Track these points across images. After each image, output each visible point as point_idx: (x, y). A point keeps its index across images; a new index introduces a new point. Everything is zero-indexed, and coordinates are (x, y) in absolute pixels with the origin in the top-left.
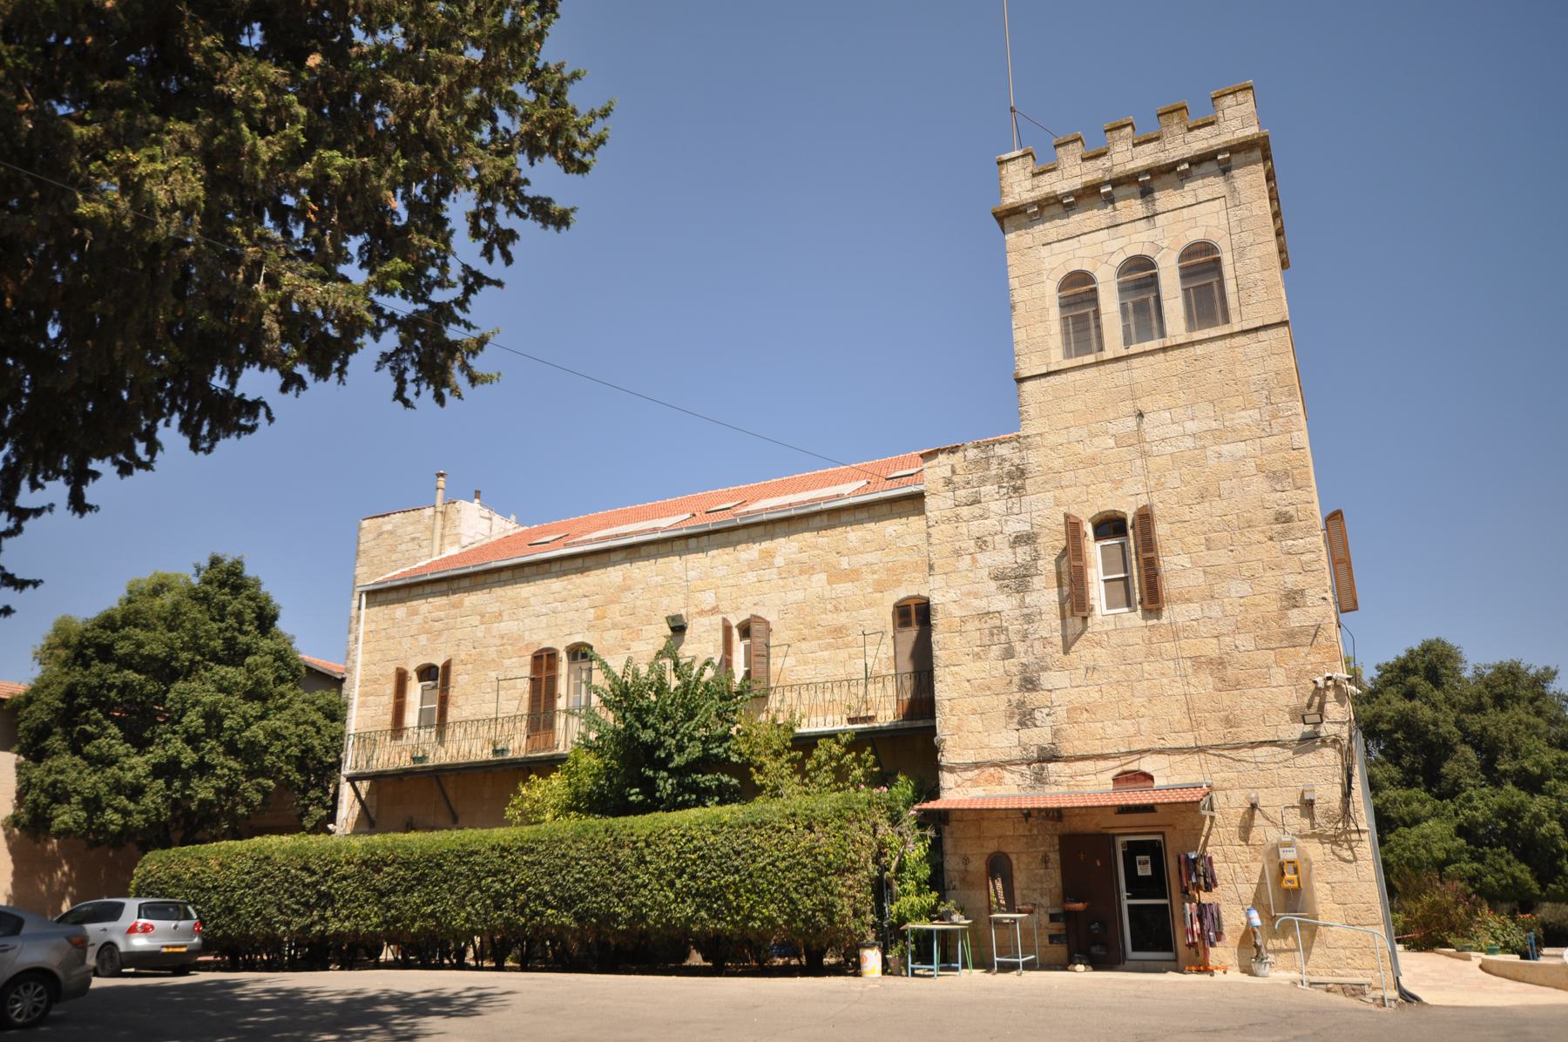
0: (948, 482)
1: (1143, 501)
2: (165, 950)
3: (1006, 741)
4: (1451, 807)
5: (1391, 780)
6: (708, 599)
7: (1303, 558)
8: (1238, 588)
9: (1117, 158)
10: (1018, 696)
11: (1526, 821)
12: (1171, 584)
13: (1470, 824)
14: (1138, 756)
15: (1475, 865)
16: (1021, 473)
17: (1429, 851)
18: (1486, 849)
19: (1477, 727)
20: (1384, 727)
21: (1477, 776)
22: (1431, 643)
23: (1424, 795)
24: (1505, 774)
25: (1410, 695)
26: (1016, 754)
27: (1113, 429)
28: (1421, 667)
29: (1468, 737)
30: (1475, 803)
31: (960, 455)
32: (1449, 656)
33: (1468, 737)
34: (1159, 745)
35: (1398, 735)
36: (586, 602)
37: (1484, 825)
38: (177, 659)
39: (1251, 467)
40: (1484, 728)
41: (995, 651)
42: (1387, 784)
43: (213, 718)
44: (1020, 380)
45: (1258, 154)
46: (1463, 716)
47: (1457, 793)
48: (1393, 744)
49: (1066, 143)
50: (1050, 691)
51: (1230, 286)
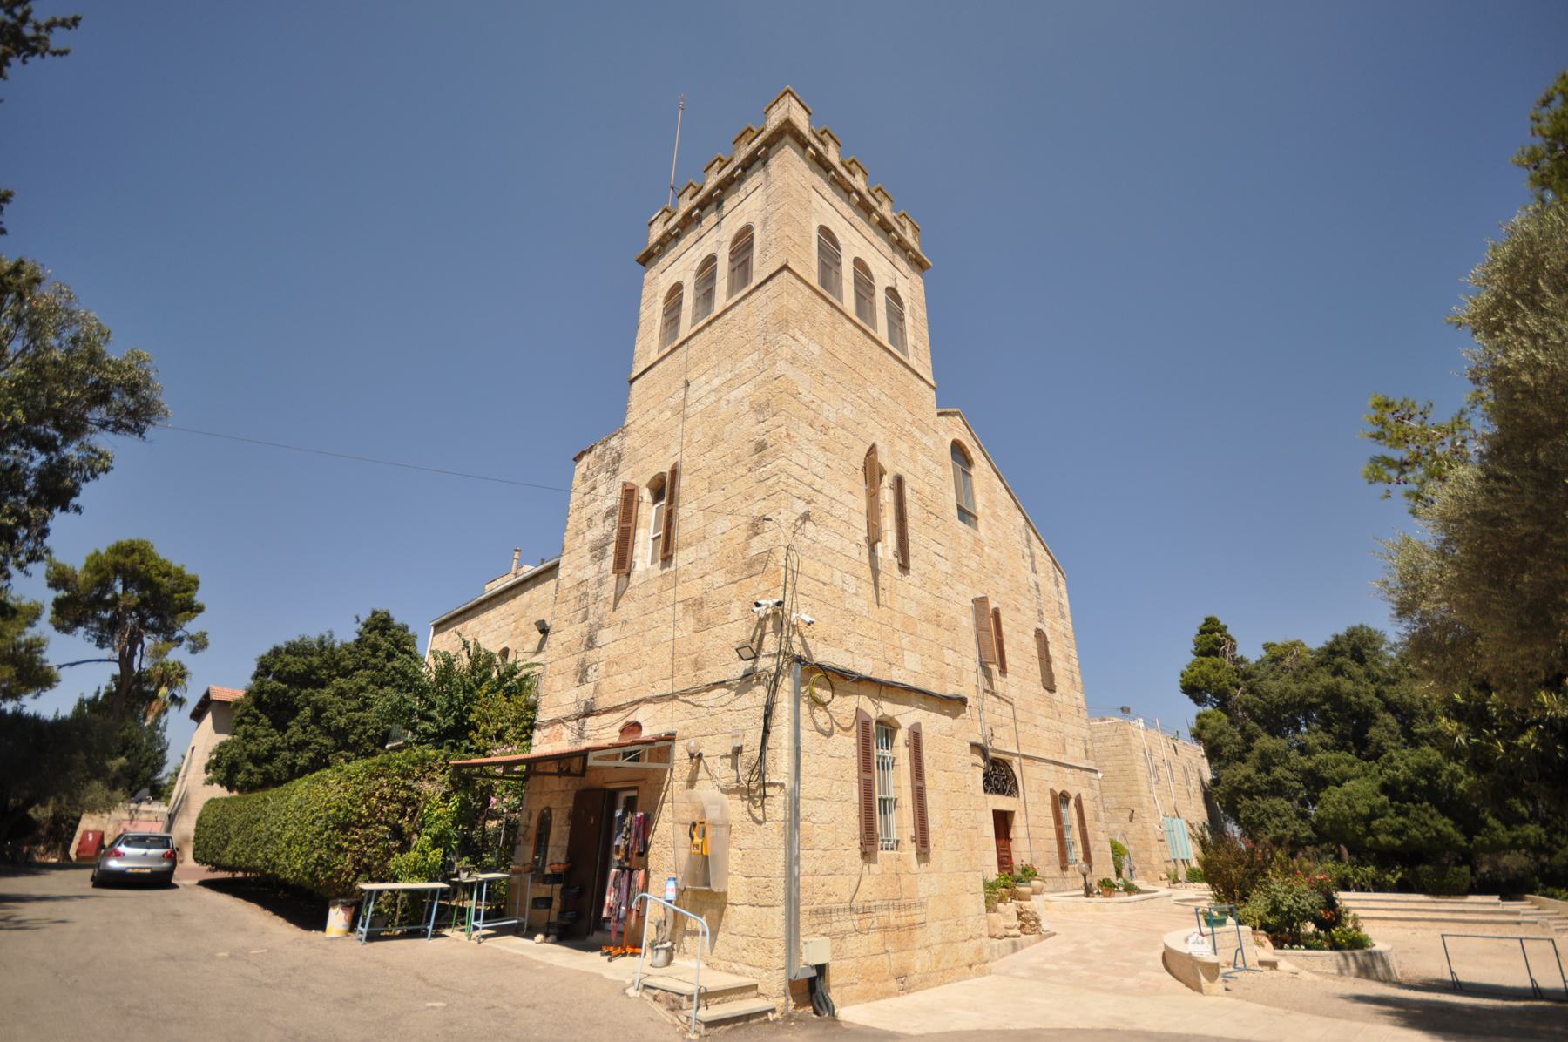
1: (677, 458)
2: (130, 871)
4: (1376, 767)
5: (1324, 746)
7: (769, 483)
8: (723, 524)
11: (1444, 778)
12: (682, 532)
13: (1393, 782)
14: (636, 706)
15: (1401, 819)
17: (1351, 807)
18: (1410, 804)
19: (1396, 696)
20: (1314, 700)
21: (1399, 739)
22: (1354, 629)
23: (1351, 757)
24: (1422, 736)
25: (1338, 671)
27: (672, 402)
28: (1348, 649)
29: (1391, 707)
30: (1395, 763)
32: (1371, 640)
33: (1391, 707)
34: (649, 695)
35: (1326, 707)
36: (512, 618)
37: (1405, 782)
38: (316, 674)
40: (1401, 697)
41: (580, 614)
42: (1320, 748)
43: (318, 711)
44: (632, 382)
45: (788, 138)
46: (1383, 687)
47: (1381, 755)
48: (1323, 714)
49: (684, 192)
50: (600, 647)
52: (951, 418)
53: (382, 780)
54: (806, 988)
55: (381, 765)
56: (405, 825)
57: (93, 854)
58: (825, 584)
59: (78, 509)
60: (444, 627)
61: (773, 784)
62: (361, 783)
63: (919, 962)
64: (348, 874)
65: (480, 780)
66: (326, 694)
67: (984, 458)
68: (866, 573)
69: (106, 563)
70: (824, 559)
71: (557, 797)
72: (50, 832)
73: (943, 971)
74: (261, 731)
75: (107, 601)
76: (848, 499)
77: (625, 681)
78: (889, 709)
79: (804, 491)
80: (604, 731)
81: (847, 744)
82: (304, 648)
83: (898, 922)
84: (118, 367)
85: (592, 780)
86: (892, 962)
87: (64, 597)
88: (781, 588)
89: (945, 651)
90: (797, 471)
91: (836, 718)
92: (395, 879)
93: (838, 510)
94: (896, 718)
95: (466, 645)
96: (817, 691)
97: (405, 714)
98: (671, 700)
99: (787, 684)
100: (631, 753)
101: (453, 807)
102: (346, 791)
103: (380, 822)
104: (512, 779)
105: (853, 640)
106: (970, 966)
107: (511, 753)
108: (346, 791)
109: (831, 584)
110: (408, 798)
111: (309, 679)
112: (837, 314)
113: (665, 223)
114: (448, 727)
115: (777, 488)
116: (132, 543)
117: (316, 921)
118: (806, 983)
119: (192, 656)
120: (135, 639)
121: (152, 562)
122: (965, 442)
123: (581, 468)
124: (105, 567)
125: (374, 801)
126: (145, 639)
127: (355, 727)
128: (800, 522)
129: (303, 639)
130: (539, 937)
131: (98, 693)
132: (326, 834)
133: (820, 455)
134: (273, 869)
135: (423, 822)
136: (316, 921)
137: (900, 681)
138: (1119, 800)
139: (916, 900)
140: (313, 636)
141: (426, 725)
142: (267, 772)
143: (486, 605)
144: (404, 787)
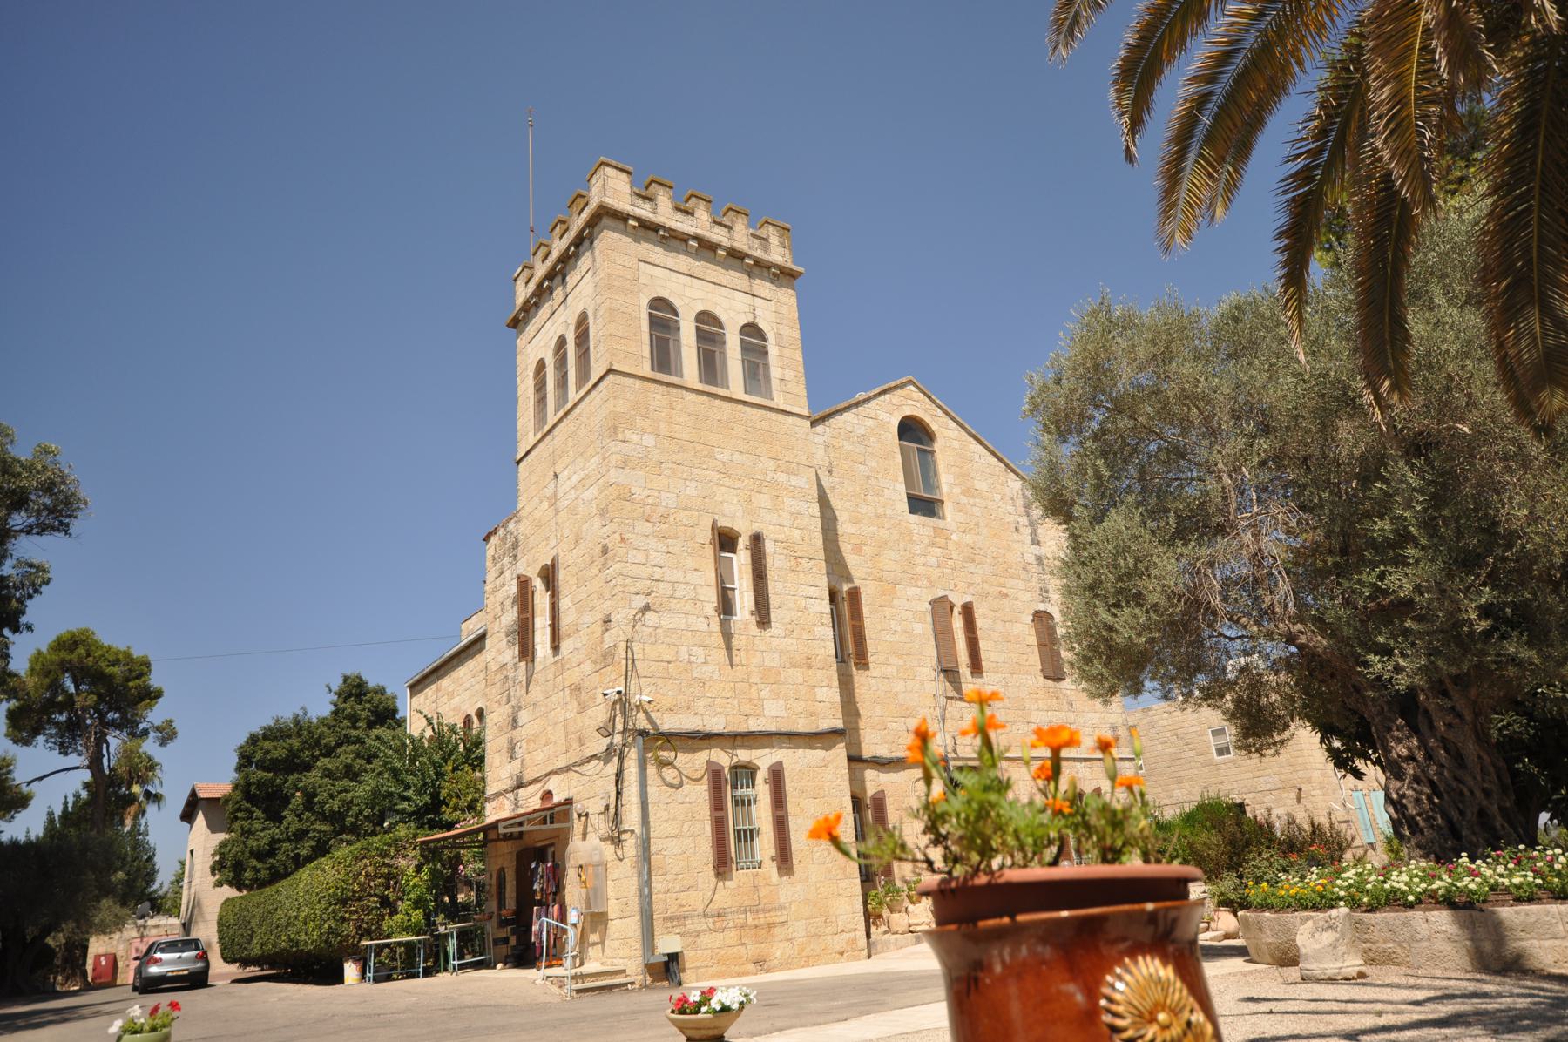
1: (553, 553)
2: (170, 974)
34: (555, 767)
38: (298, 757)
43: (309, 797)
44: (518, 463)
45: (606, 221)
52: (899, 392)
53: (365, 861)
54: (663, 969)
55: (362, 849)
56: (390, 895)
57: (109, 979)
58: (669, 662)
59: (29, 628)
60: (419, 687)
61: (625, 831)
62: (350, 866)
63: (778, 951)
64: (354, 937)
65: (446, 851)
66: (313, 778)
67: (954, 425)
68: (718, 640)
69: (52, 663)
70: (665, 641)
71: (504, 857)
72: (66, 960)
73: (808, 957)
74: (257, 825)
75: (60, 703)
76: (694, 578)
77: (539, 756)
78: (743, 755)
79: (643, 585)
80: (530, 800)
81: (700, 793)
82: (280, 730)
83: (756, 922)
84: (30, 468)
85: (527, 840)
86: (752, 950)
87: (18, 708)
88: (623, 677)
89: (817, 690)
90: (634, 570)
91: (685, 773)
92: (388, 937)
93: (681, 591)
94: (754, 761)
95: (430, 723)
96: (661, 753)
97: (385, 797)
98: (567, 771)
99: (632, 755)
100: (535, 819)
101: (425, 874)
102: (339, 873)
103: (371, 896)
104: (475, 847)
105: (702, 703)
106: (842, 954)
107: (469, 823)
108: (339, 873)
109: (677, 660)
110: (389, 873)
111: (292, 764)
112: (675, 390)
113: (527, 283)
114: (426, 804)
115: (616, 591)
116: (73, 635)
117: (336, 978)
118: (662, 966)
119: (163, 749)
120: (101, 740)
121: (99, 653)
122: (921, 415)
123: (490, 550)
124: (52, 668)
125: (362, 879)
126: (108, 738)
127: (349, 809)
128: (640, 615)
129: (278, 720)
130: (500, 966)
131: (66, 803)
132: (331, 909)
133: (662, 547)
134: (297, 946)
135: (404, 891)
136: (336, 978)
137: (759, 729)
138: (1283, 777)
139: (777, 905)
140: (287, 715)
141: (405, 805)
142: (272, 867)
143: (455, 661)
144: (384, 865)
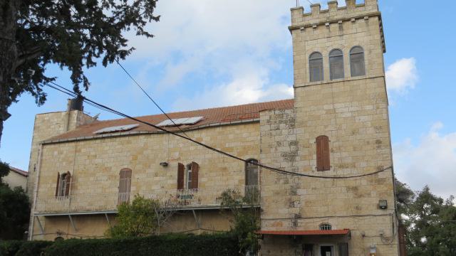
0: (268, 121)
3: (284, 211)
6: (177, 155)
9: (332, 14)
10: (289, 197)
16: (293, 120)
26: (287, 216)
31: (273, 112)
39: (369, 124)
51: (366, 62)
